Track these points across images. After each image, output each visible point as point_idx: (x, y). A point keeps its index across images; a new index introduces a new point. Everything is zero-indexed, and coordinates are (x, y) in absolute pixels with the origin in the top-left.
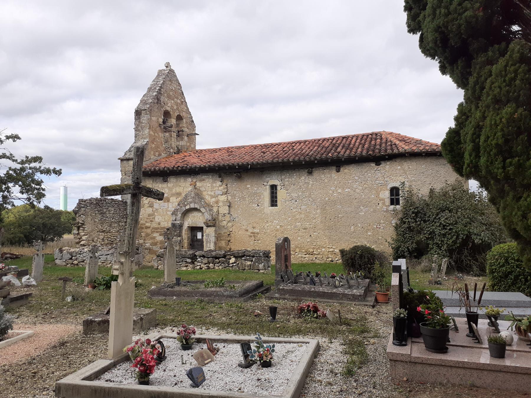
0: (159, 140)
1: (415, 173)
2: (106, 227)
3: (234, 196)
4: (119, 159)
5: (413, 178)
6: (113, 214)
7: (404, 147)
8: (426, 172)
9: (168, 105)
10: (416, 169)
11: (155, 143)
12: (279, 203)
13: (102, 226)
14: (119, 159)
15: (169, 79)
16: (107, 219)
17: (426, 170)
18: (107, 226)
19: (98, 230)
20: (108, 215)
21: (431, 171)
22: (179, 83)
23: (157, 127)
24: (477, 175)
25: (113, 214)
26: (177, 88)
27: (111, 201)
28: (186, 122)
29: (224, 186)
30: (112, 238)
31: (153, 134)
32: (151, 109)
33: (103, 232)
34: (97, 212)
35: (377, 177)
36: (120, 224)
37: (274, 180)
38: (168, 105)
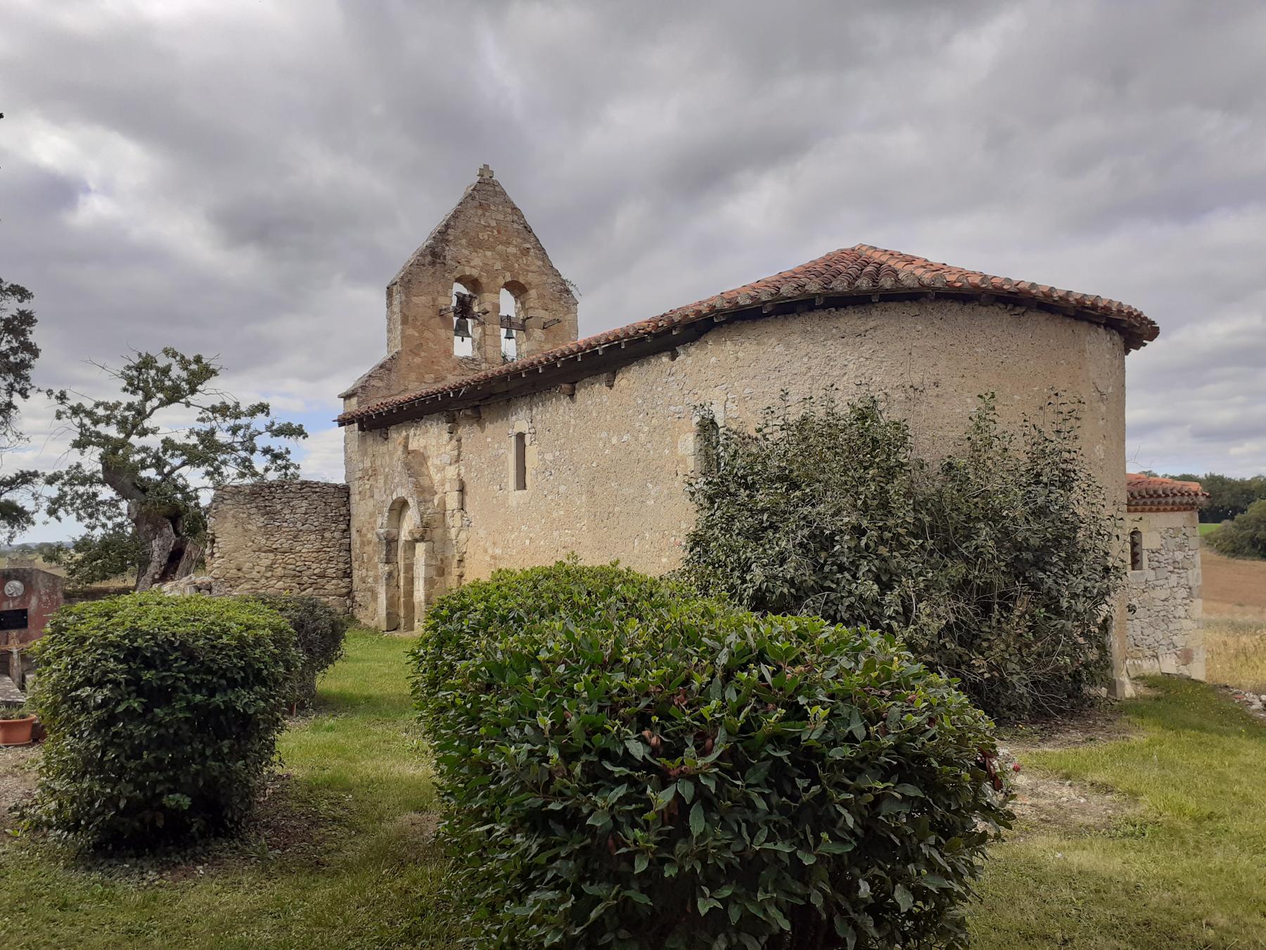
0: (437, 347)
1: (752, 375)
2: (282, 541)
3: (469, 468)
4: (340, 397)
5: (747, 391)
6: (306, 514)
7: (909, 276)
8: (787, 366)
9: (472, 264)
10: (757, 360)
11: (423, 354)
12: (528, 488)
13: (267, 539)
14: (340, 397)
15: (477, 204)
16: (285, 524)
17: (788, 358)
18: (284, 540)
19: (255, 547)
20: (287, 517)
21: (805, 359)
22: (515, 209)
23: (431, 318)
24: (194, 367)
25: (306, 514)
26: (508, 219)
27: (299, 487)
28: (541, 296)
29: (454, 442)
30: (298, 564)
31: (417, 334)
32: (409, 281)
33: (271, 551)
34: (253, 511)
35: (670, 394)
36: (327, 535)
37: (520, 421)
38: (472, 264)
